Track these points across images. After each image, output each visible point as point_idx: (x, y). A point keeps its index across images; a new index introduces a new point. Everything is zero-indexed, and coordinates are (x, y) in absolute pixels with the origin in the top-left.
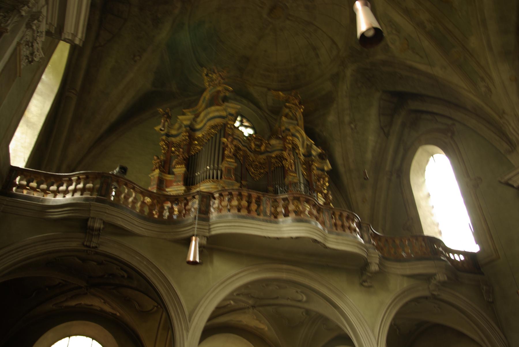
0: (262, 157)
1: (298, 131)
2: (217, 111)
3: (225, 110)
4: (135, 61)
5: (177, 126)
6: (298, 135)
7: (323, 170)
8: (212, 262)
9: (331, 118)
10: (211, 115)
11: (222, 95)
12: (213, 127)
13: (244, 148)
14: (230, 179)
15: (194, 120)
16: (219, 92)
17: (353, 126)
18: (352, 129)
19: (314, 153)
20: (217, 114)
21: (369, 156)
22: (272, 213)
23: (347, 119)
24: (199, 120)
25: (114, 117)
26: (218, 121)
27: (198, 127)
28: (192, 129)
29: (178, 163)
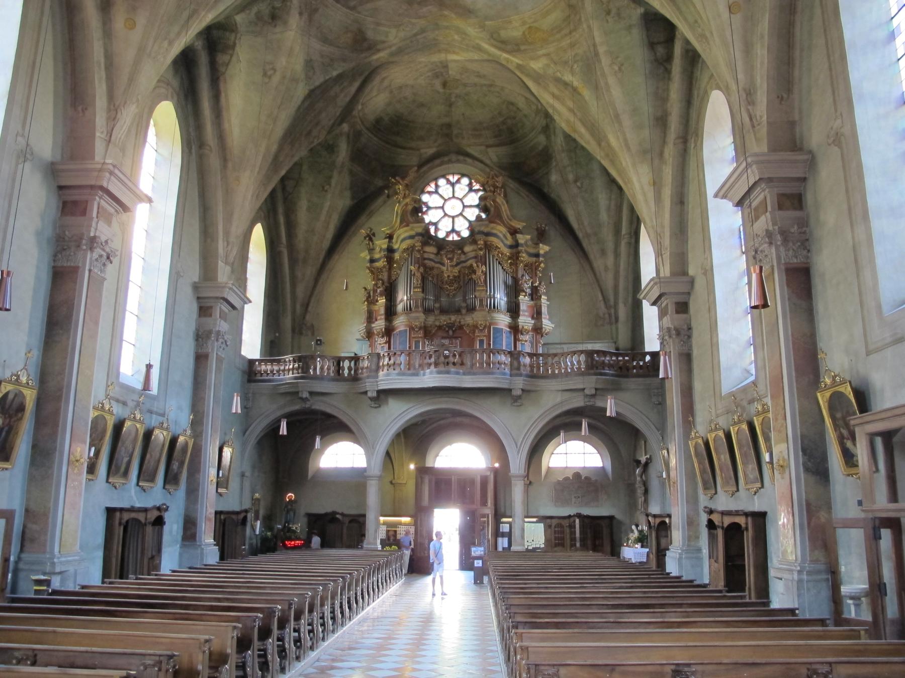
0: (456, 270)
1: (492, 228)
2: (406, 231)
3: (412, 229)
4: (326, 191)
5: (378, 249)
6: (494, 231)
7: (537, 255)
8: (387, 404)
9: (554, 177)
10: (402, 236)
11: (410, 208)
12: (405, 250)
13: (437, 265)
14: (417, 312)
15: (390, 242)
16: (406, 205)
17: (579, 184)
18: (579, 188)
19: (521, 241)
20: (407, 234)
21: (604, 216)
22: (420, 365)
23: (571, 177)
24: (394, 240)
25: (326, 244)
26: (409, 242)
27: (396, 247)
28: (390, 250)
29: (381, 295)
